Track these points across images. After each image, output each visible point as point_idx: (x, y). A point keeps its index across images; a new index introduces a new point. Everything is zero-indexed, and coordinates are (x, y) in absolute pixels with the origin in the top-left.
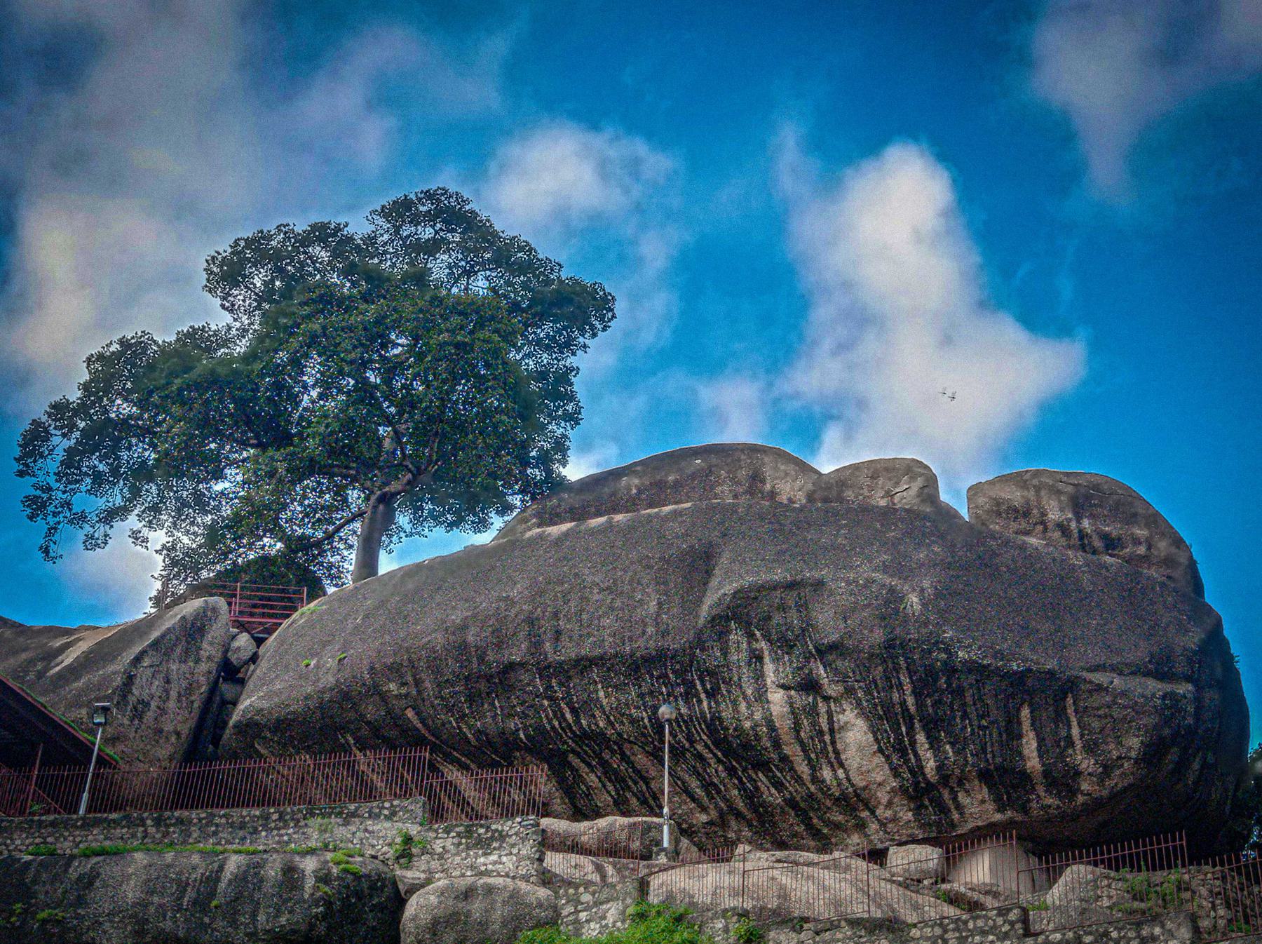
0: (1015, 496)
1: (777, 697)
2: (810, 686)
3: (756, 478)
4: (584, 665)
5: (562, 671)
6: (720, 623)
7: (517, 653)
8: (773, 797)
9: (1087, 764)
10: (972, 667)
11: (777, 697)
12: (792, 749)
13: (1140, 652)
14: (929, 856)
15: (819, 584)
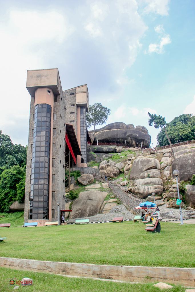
0: (139, 127)
1: (130, 140)
2: (132, 140)
3: (123, 125)
4: (120, 138)
5: (119, 138)
6: (127, 136)
7: (116, 137)
8: (129, 145)
9: (145, 143)
10: (140, 139)
11: (130, 140)
12: (130, 143)
13: (147, 138)
14: (137, 148)
15: (133, 135)
